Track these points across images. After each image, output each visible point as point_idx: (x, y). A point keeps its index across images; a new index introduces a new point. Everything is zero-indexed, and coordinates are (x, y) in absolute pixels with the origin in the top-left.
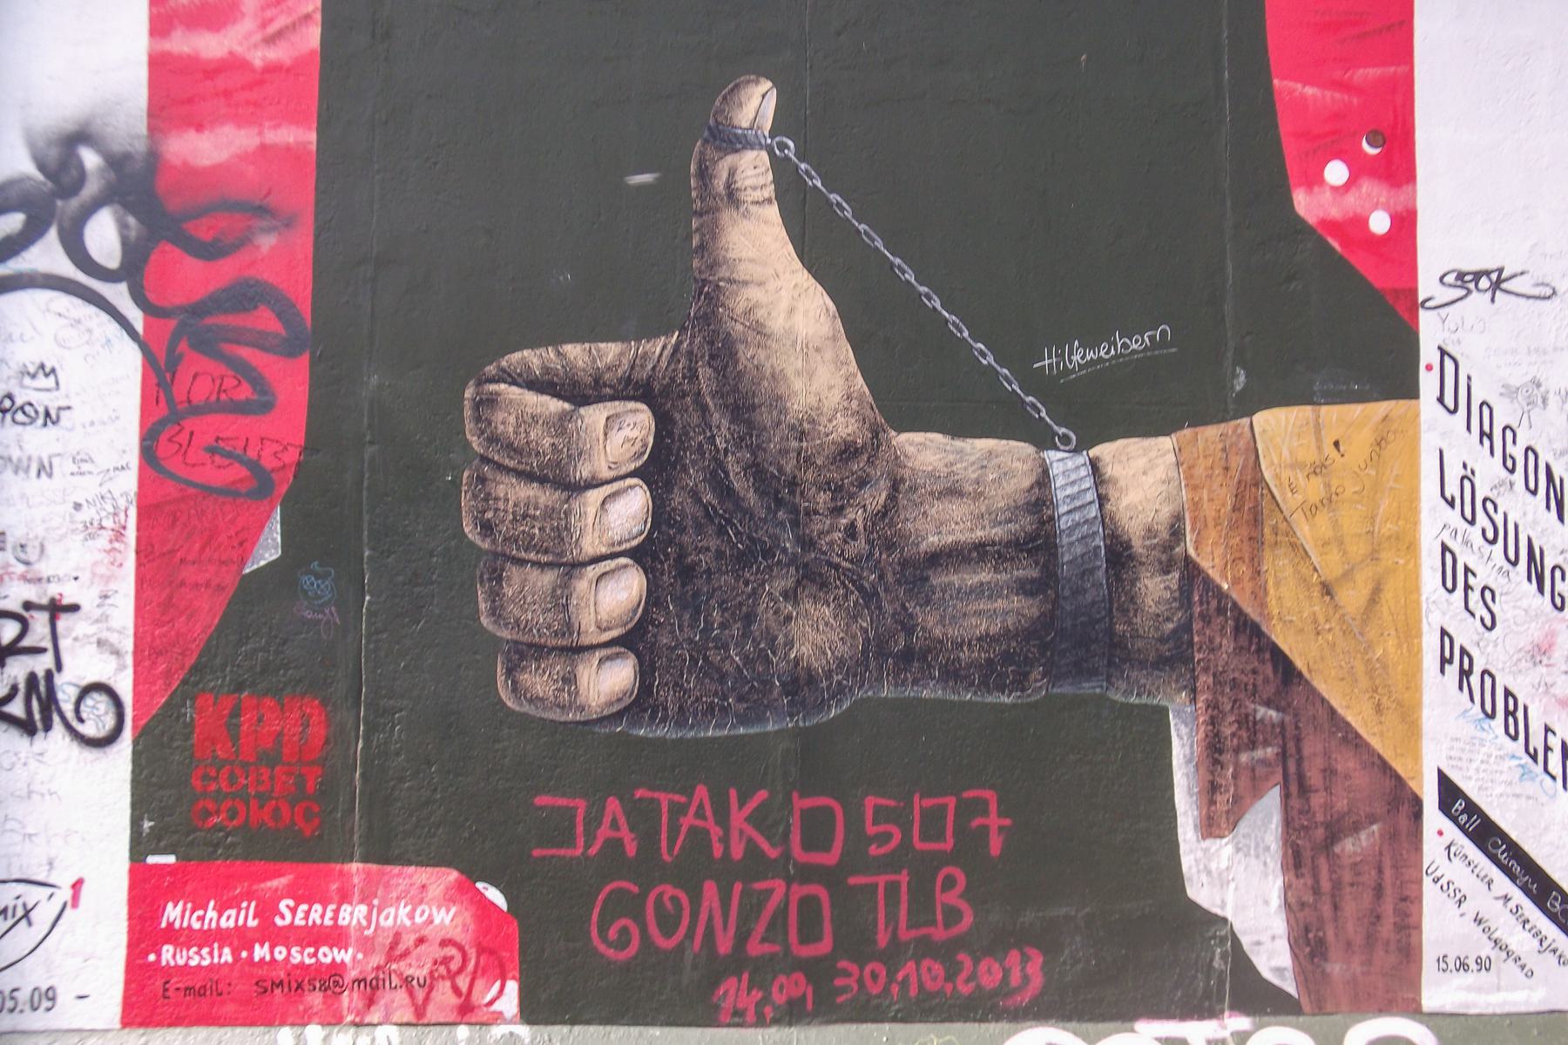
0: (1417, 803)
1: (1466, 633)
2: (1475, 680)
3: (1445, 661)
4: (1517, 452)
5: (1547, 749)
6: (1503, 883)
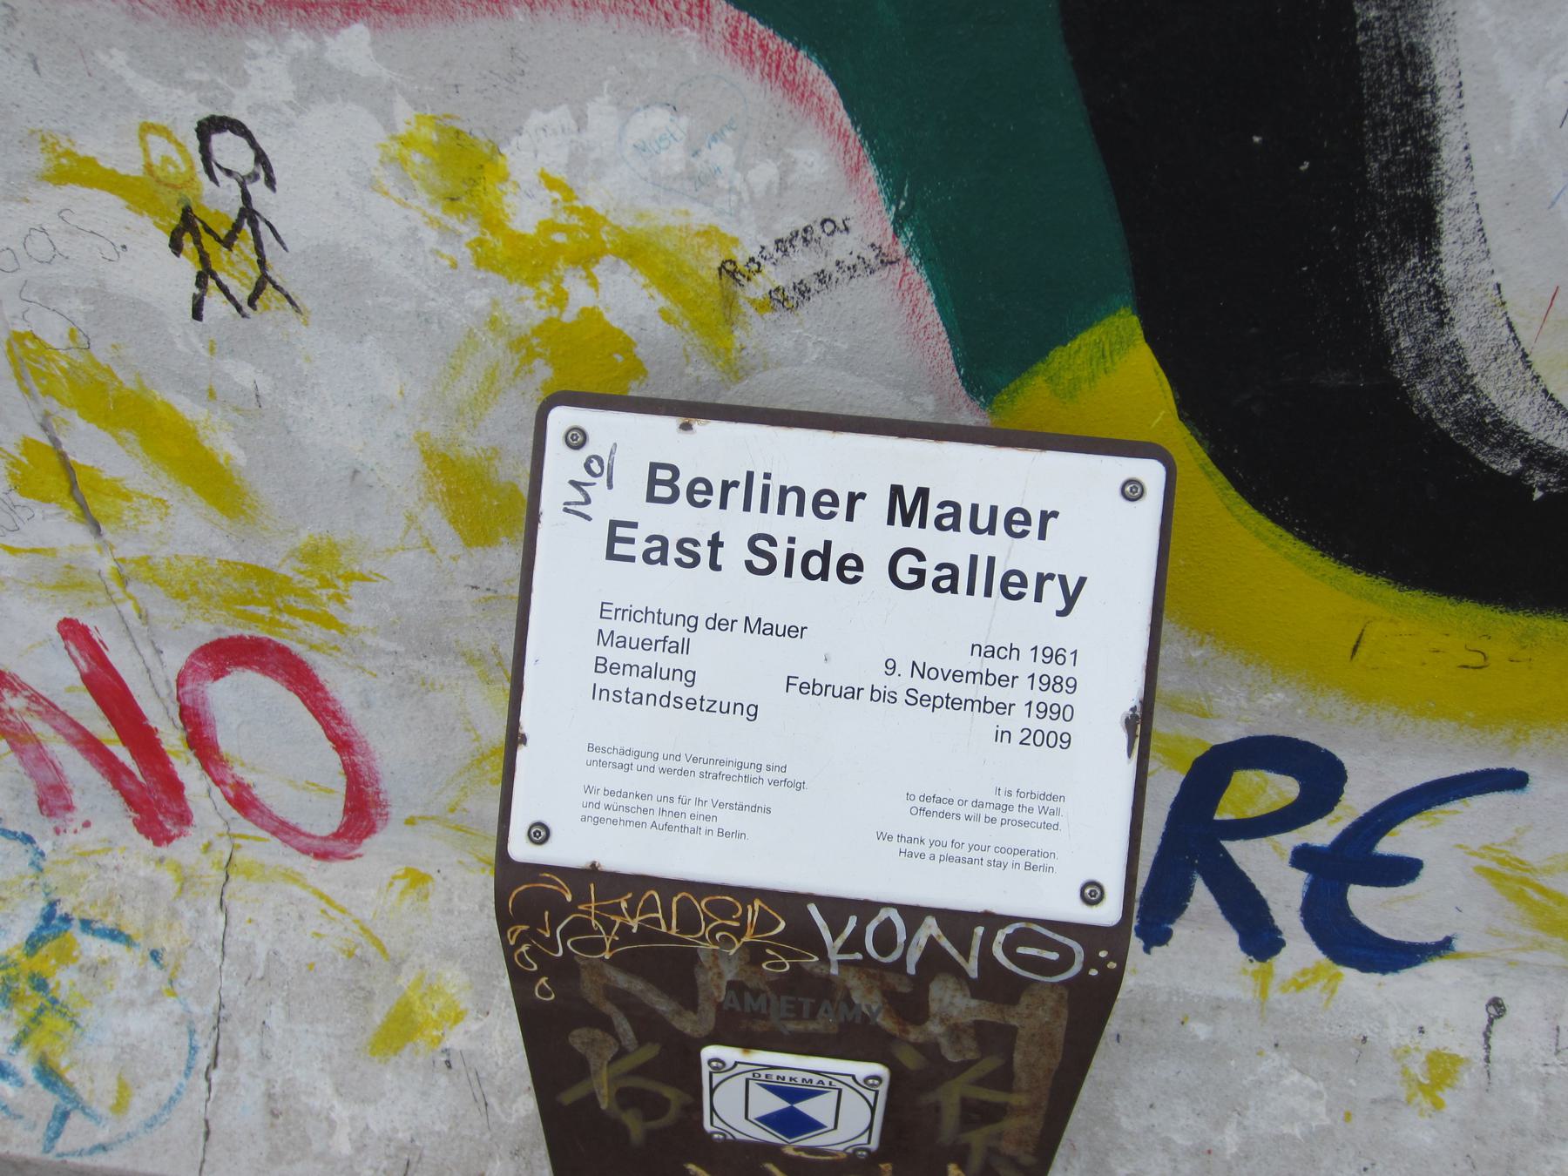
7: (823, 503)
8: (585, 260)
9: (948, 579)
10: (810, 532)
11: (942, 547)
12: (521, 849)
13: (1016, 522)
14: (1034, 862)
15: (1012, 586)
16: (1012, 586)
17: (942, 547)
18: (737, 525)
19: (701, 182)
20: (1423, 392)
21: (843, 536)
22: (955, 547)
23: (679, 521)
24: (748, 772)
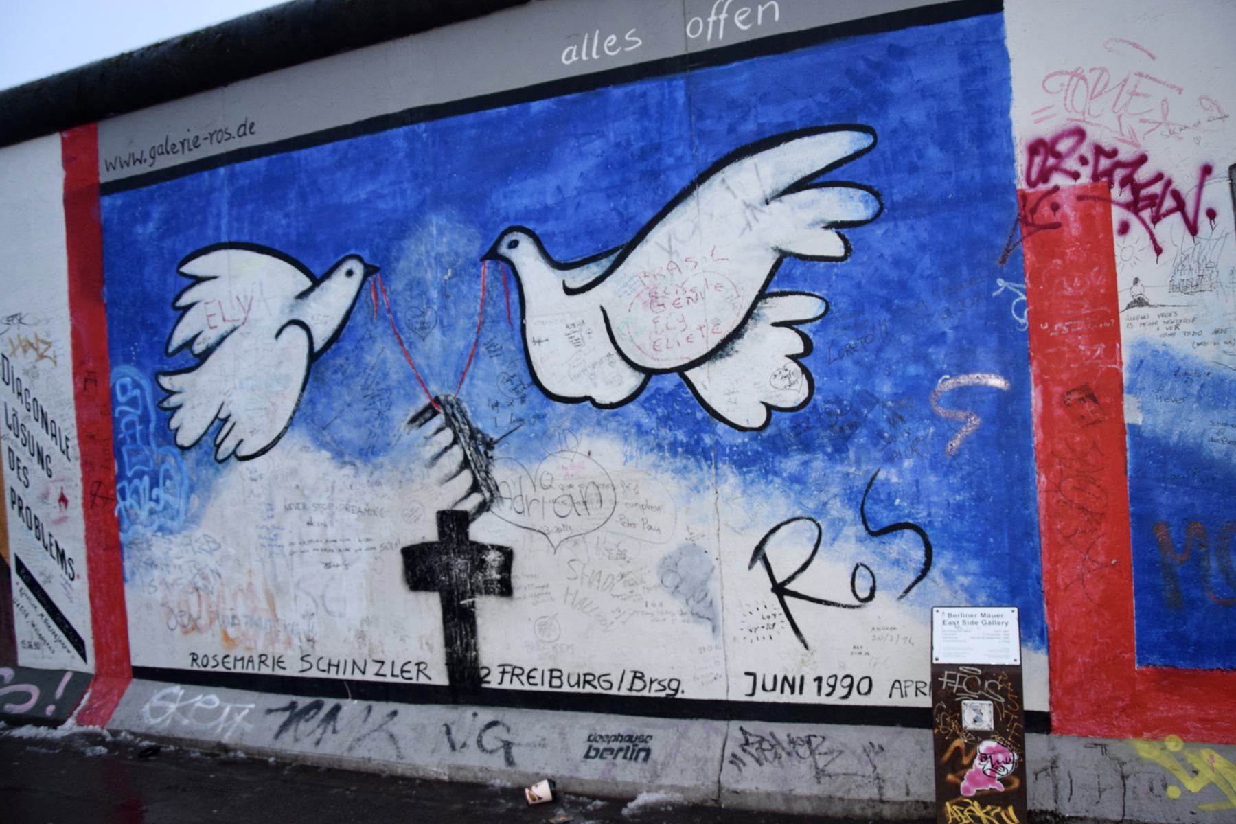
0: (8, 569)
1: (20, 490)
2: (24, 511)
3: (14, 503)
4: (30, 401)
5: (51, 545)
6: (41, 610)
7: (972, 616)
9: (990, 623)
10: (970, 619)
11: (988, 620)
12: (935, 662)
13: (998, 616)
14: (1007, 657)
15: (998, 623)
16: (998, 623)
17: (988, 620)
18: (960, 619)
21: (975, 620)
22: (991, 619)
23: (953, 619)
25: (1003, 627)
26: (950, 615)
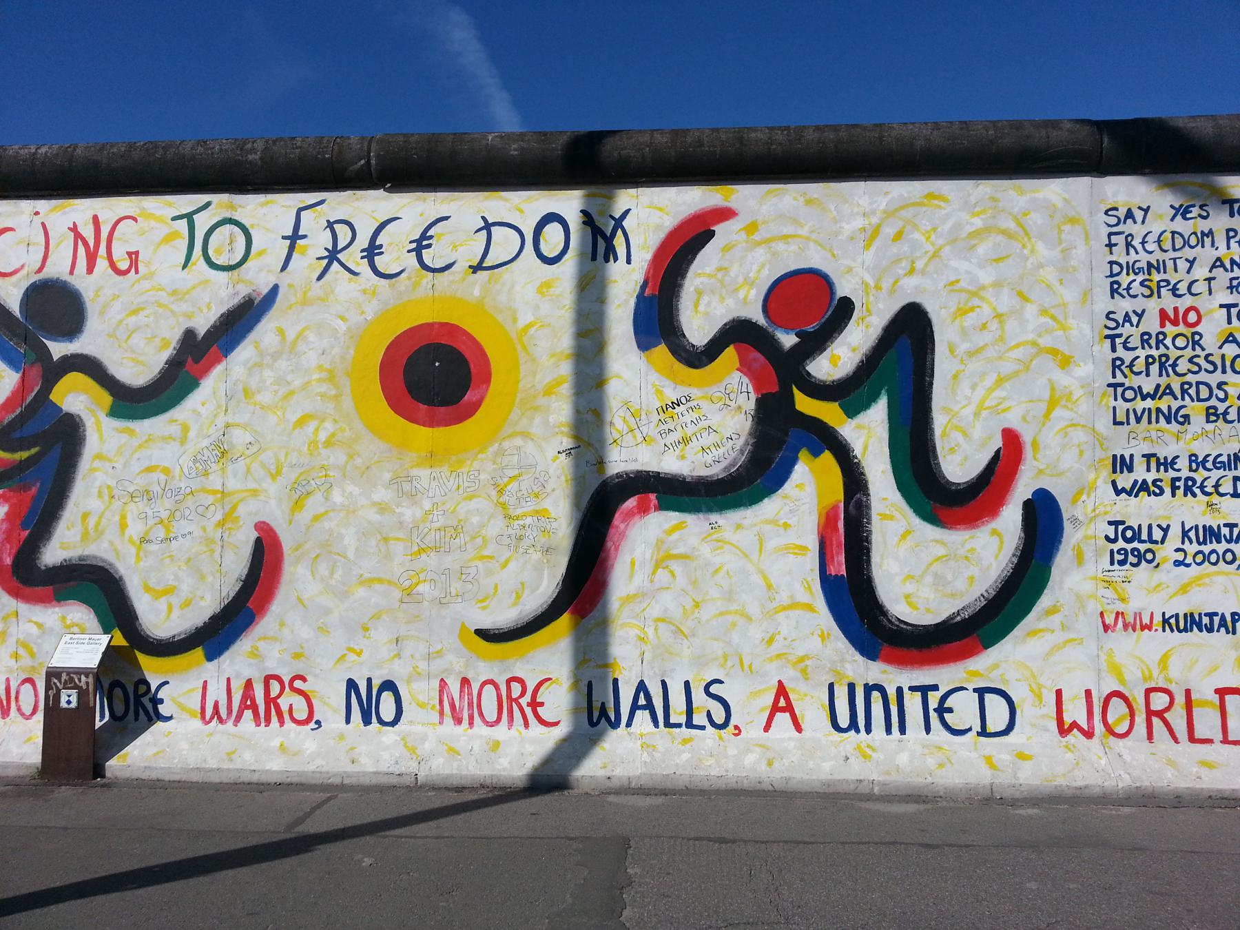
8: (73, 626)
10: (82, 641)
11: (91, 641)
13: (98, 640)
15: (96, 644)
16: (96, 644)
18: (76, 641)
19: (82, 619)
20: (142, 633)
21: (84, 641)
23: (71, 641)
24: (70, 658)
25: (98, 646)
26: (71, 639)
